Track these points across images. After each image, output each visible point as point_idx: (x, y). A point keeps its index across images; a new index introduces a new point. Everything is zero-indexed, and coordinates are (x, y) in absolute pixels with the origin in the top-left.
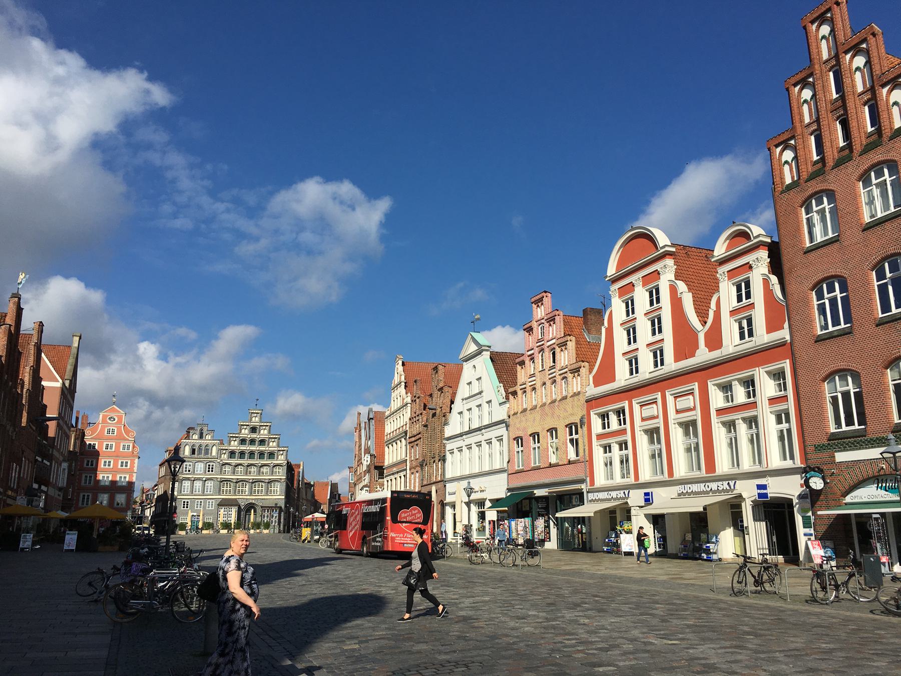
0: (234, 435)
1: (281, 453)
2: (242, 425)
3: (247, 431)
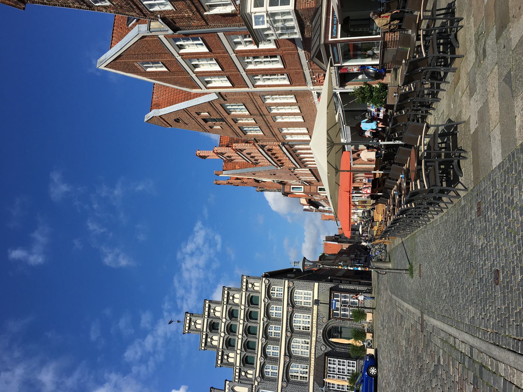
0: (220, 358)
1: (250, 286)
2: (206, 344)
3: (215, 338)
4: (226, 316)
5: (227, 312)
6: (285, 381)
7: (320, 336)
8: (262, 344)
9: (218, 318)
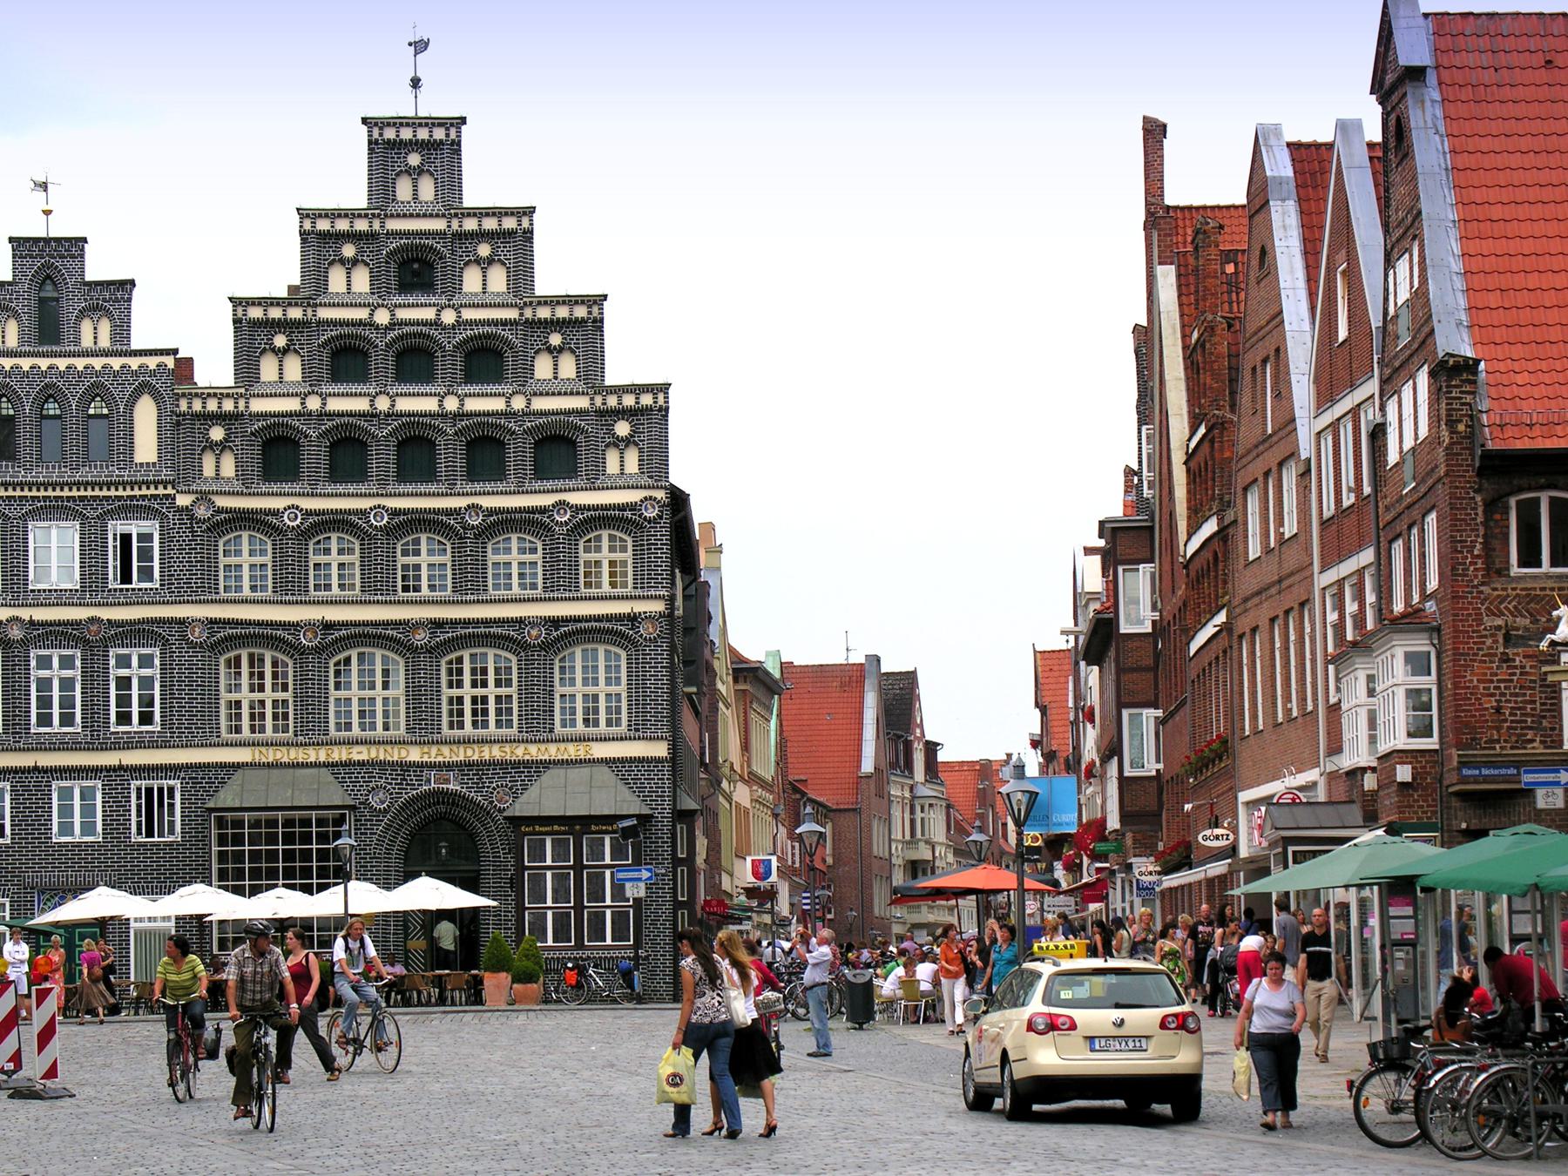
1: (622, 429)
4: (471, 323)
7: (429, 781)
9: (455, 287)
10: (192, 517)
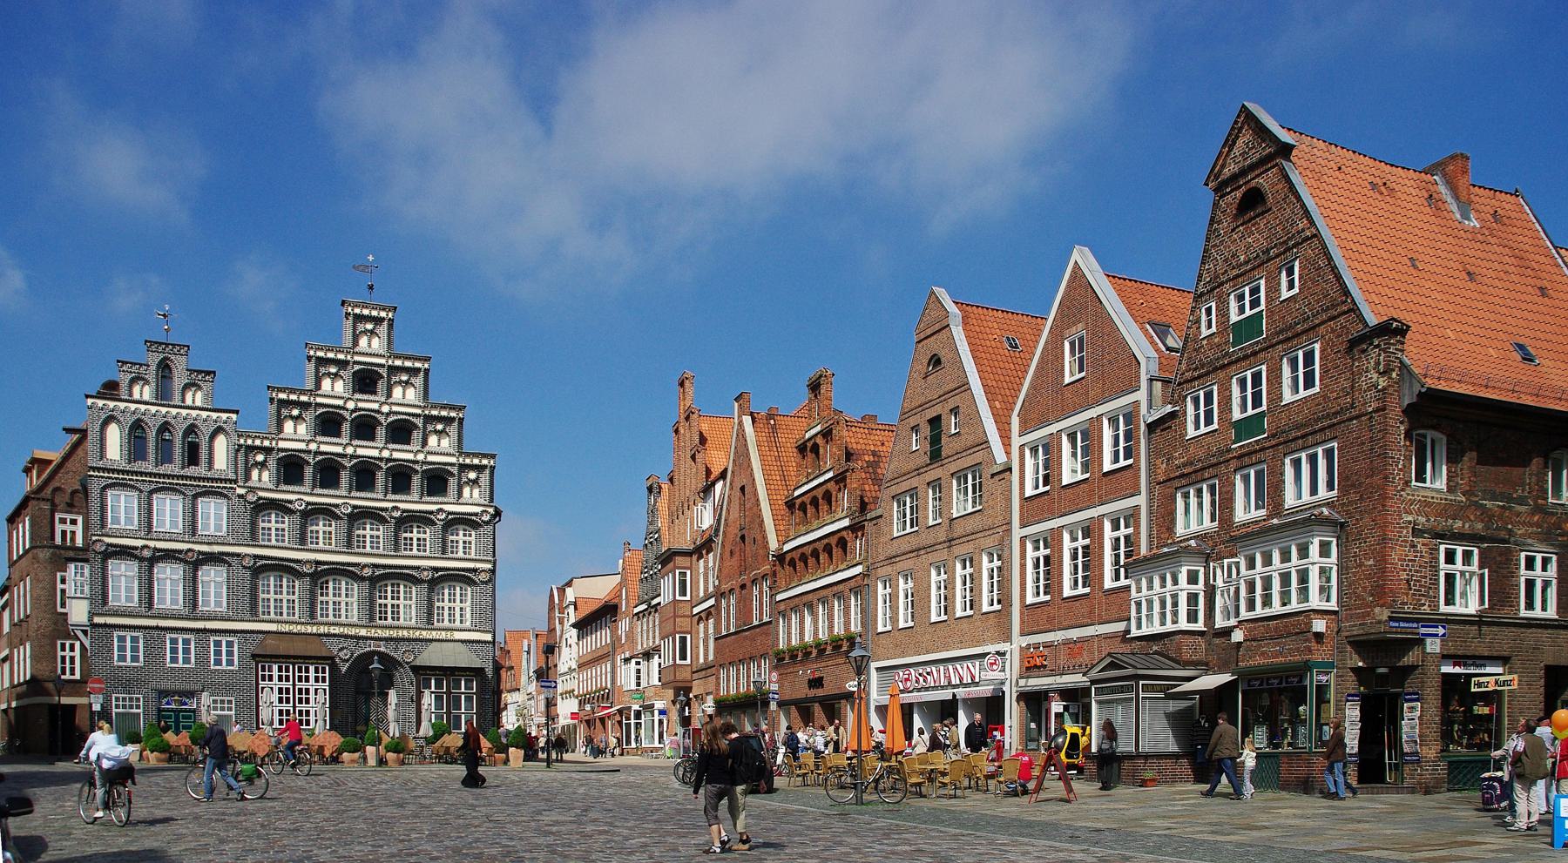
5: (404, 417)
6: (255, 563)
7: (370, 646)
8: (337, 506)
10: (245, 501)
